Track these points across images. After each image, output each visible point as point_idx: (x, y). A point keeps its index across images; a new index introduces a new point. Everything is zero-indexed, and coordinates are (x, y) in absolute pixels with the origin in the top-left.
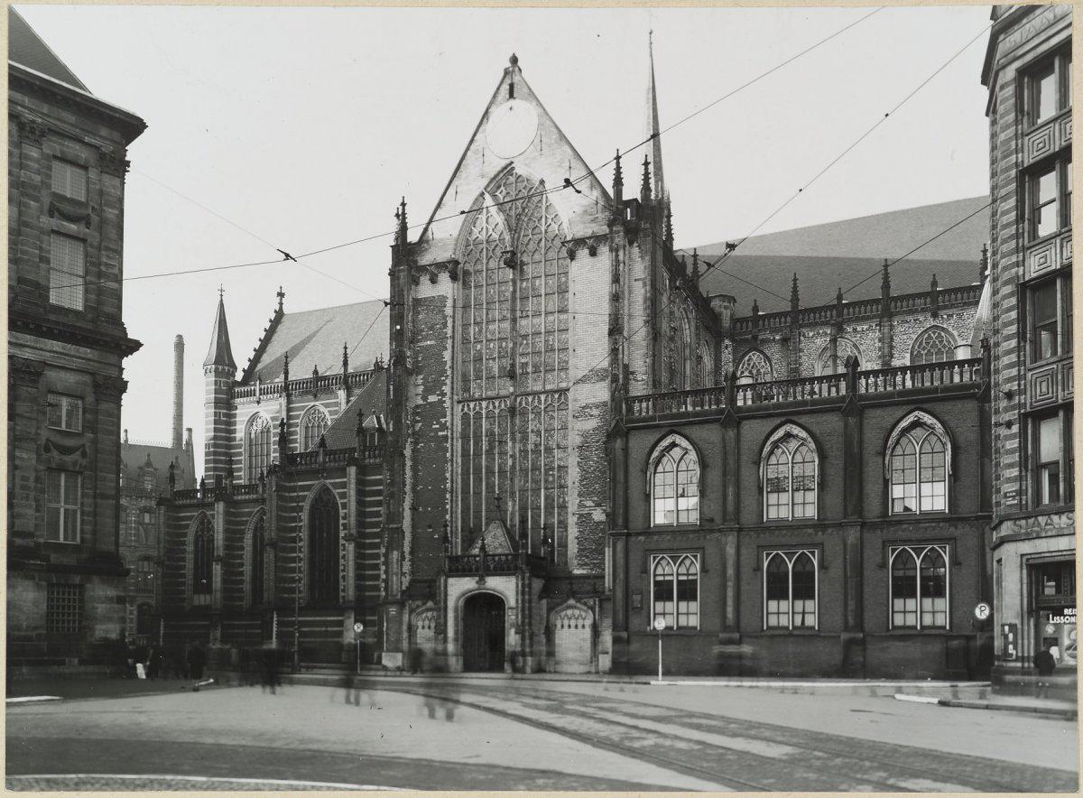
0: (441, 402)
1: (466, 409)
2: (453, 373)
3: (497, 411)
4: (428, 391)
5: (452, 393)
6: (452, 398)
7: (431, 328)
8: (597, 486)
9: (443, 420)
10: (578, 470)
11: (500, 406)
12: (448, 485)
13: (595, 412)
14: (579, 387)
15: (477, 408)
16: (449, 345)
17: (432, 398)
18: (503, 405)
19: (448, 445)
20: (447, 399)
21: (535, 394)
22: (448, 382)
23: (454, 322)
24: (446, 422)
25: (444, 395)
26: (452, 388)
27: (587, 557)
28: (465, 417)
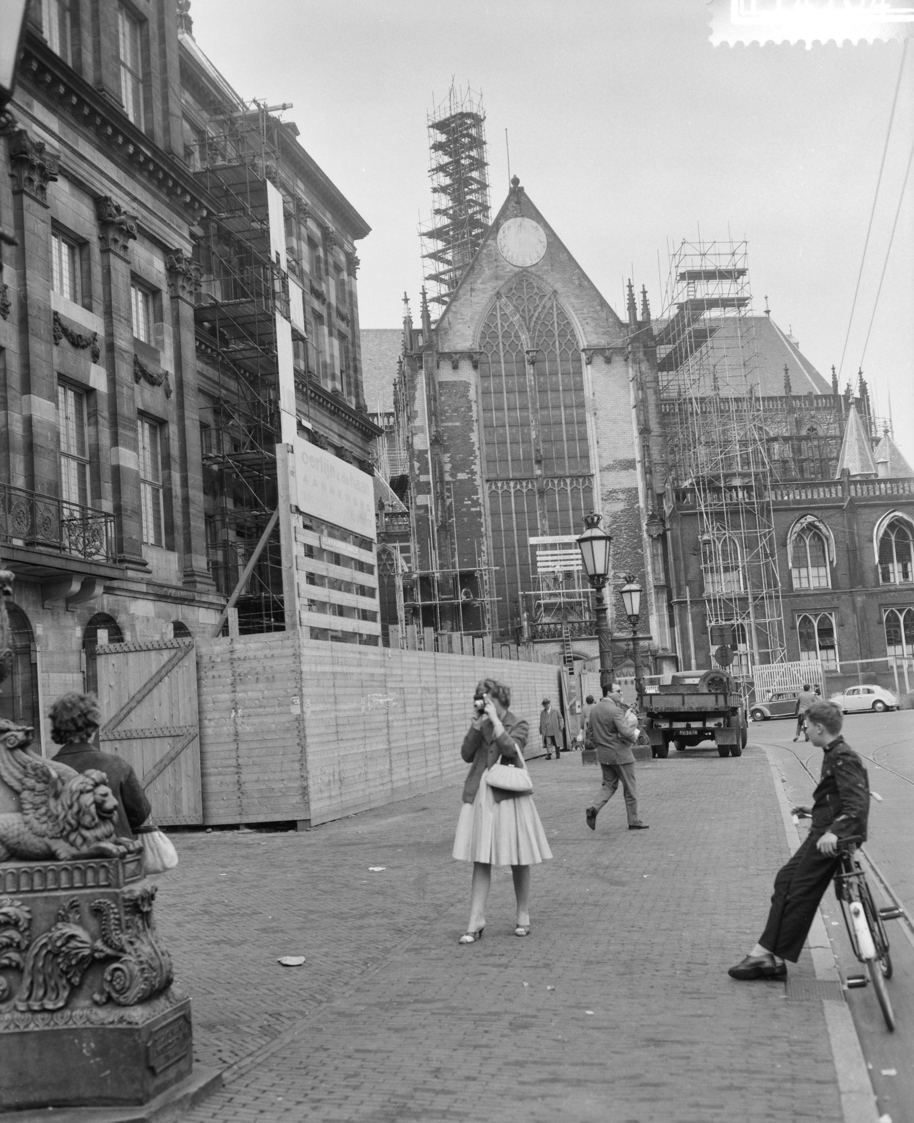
1: (493, 487)
3: (525, 491)
4: (456, 469)
6: (481, 477)
7: (456, 410)
8: (629, 560)
9: (475, 497)
11: (527, 486)
13: (621, 496)
14: (605, 473)
15: (505, 487)
16: (475, 428)
17: (462, 476)
20: (477, 477)
21: (561, 478)
22: (477, 461)
24: (478, 499)
25: (473, 473)
28: (493, 495)
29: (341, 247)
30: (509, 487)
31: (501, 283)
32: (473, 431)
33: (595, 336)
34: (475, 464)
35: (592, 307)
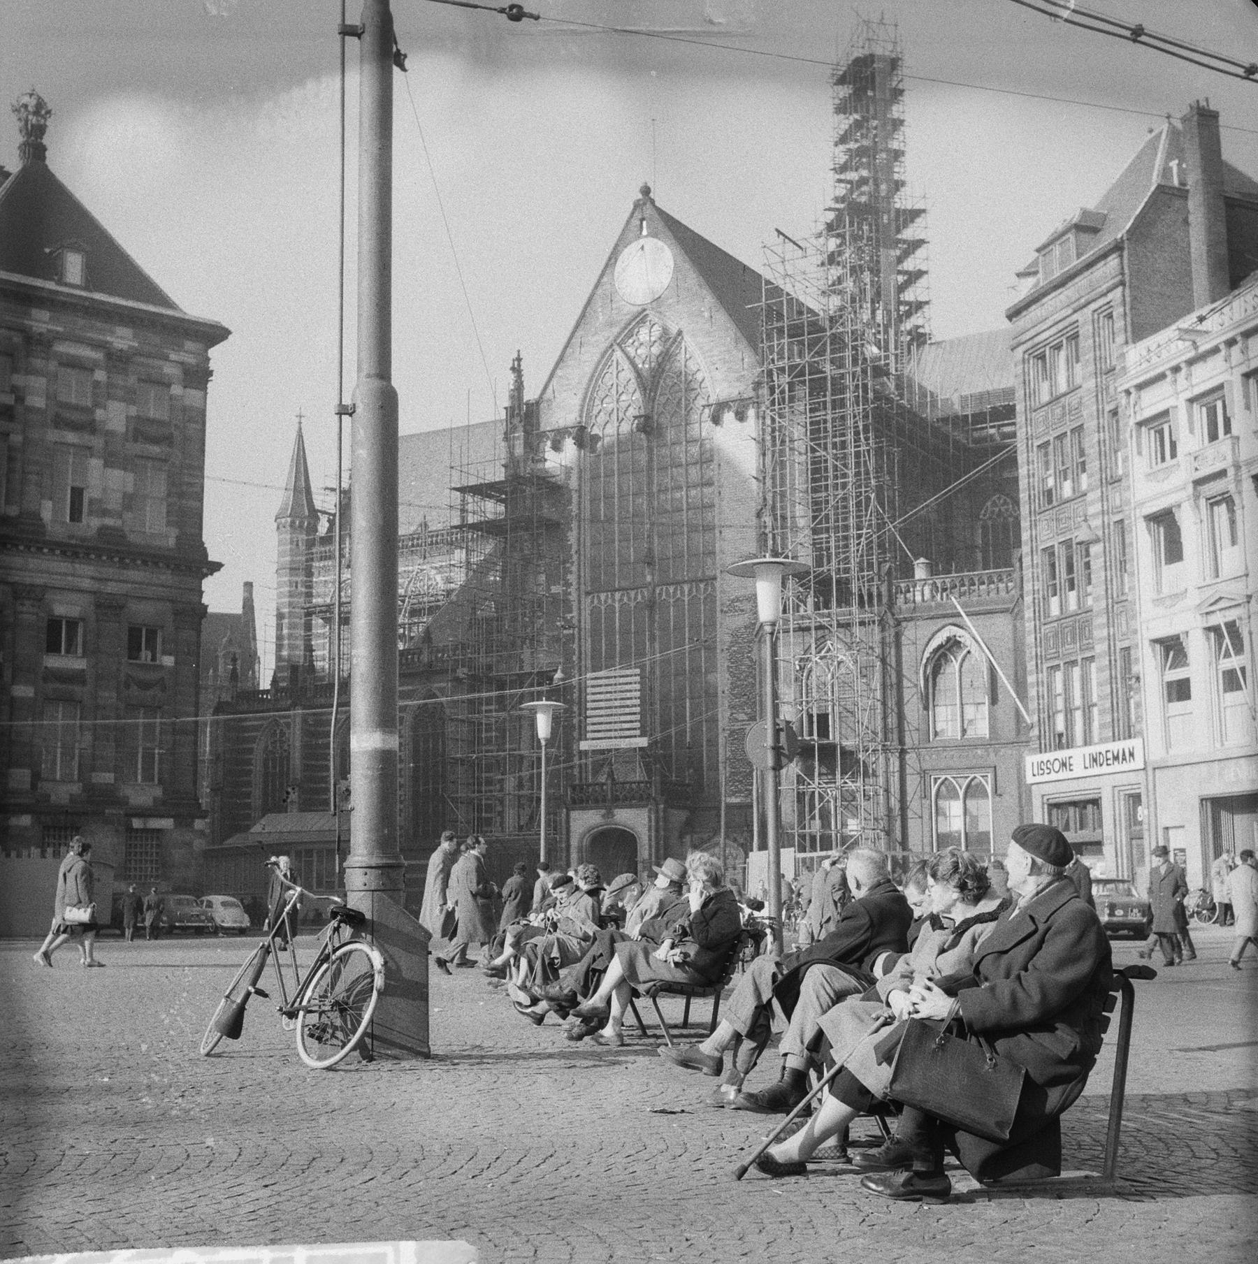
0: (566, 593)
2: (579, 558)
3: (632, 604)
5: (579, 583)
9: (569, 616)
10: (727, 676)
11: (636, 598)
12: (576, 696)
16: (574, 525)
17: (555, 589)
18: (639, 597)
19: (575, 646)
20: (572, 589)
22: (574, 569)
23: (580, 497)
25: (568, 584)
26: (579, 577)
27: (741, 782)
28: (595, 612)
29: (166, 359)
30: (614, 600)
31: (616, 330)
32: (571, 529)
33: (726, 385)
34: (571, 572)
35: (724, 345)
